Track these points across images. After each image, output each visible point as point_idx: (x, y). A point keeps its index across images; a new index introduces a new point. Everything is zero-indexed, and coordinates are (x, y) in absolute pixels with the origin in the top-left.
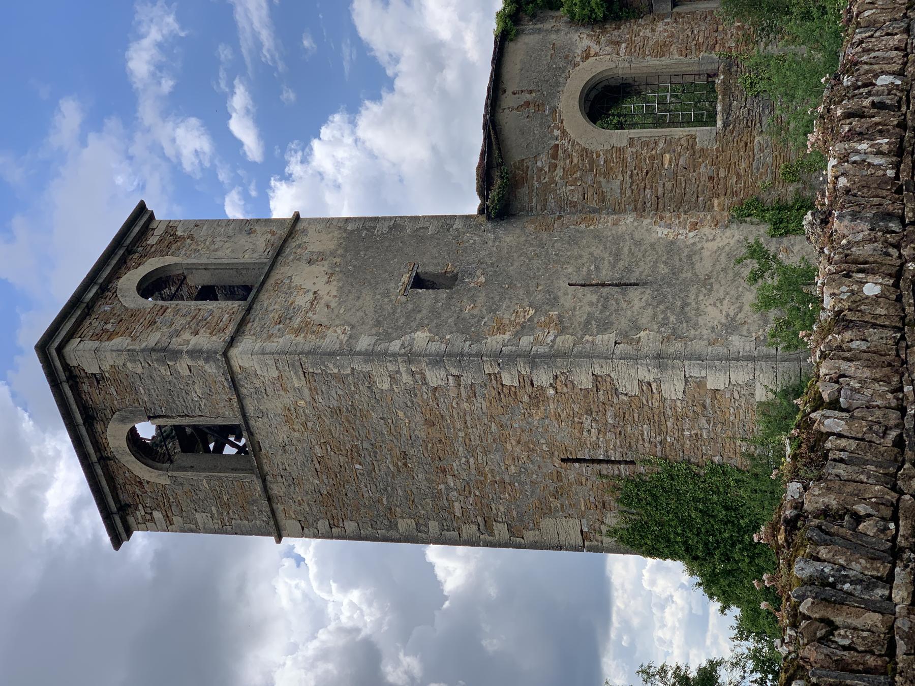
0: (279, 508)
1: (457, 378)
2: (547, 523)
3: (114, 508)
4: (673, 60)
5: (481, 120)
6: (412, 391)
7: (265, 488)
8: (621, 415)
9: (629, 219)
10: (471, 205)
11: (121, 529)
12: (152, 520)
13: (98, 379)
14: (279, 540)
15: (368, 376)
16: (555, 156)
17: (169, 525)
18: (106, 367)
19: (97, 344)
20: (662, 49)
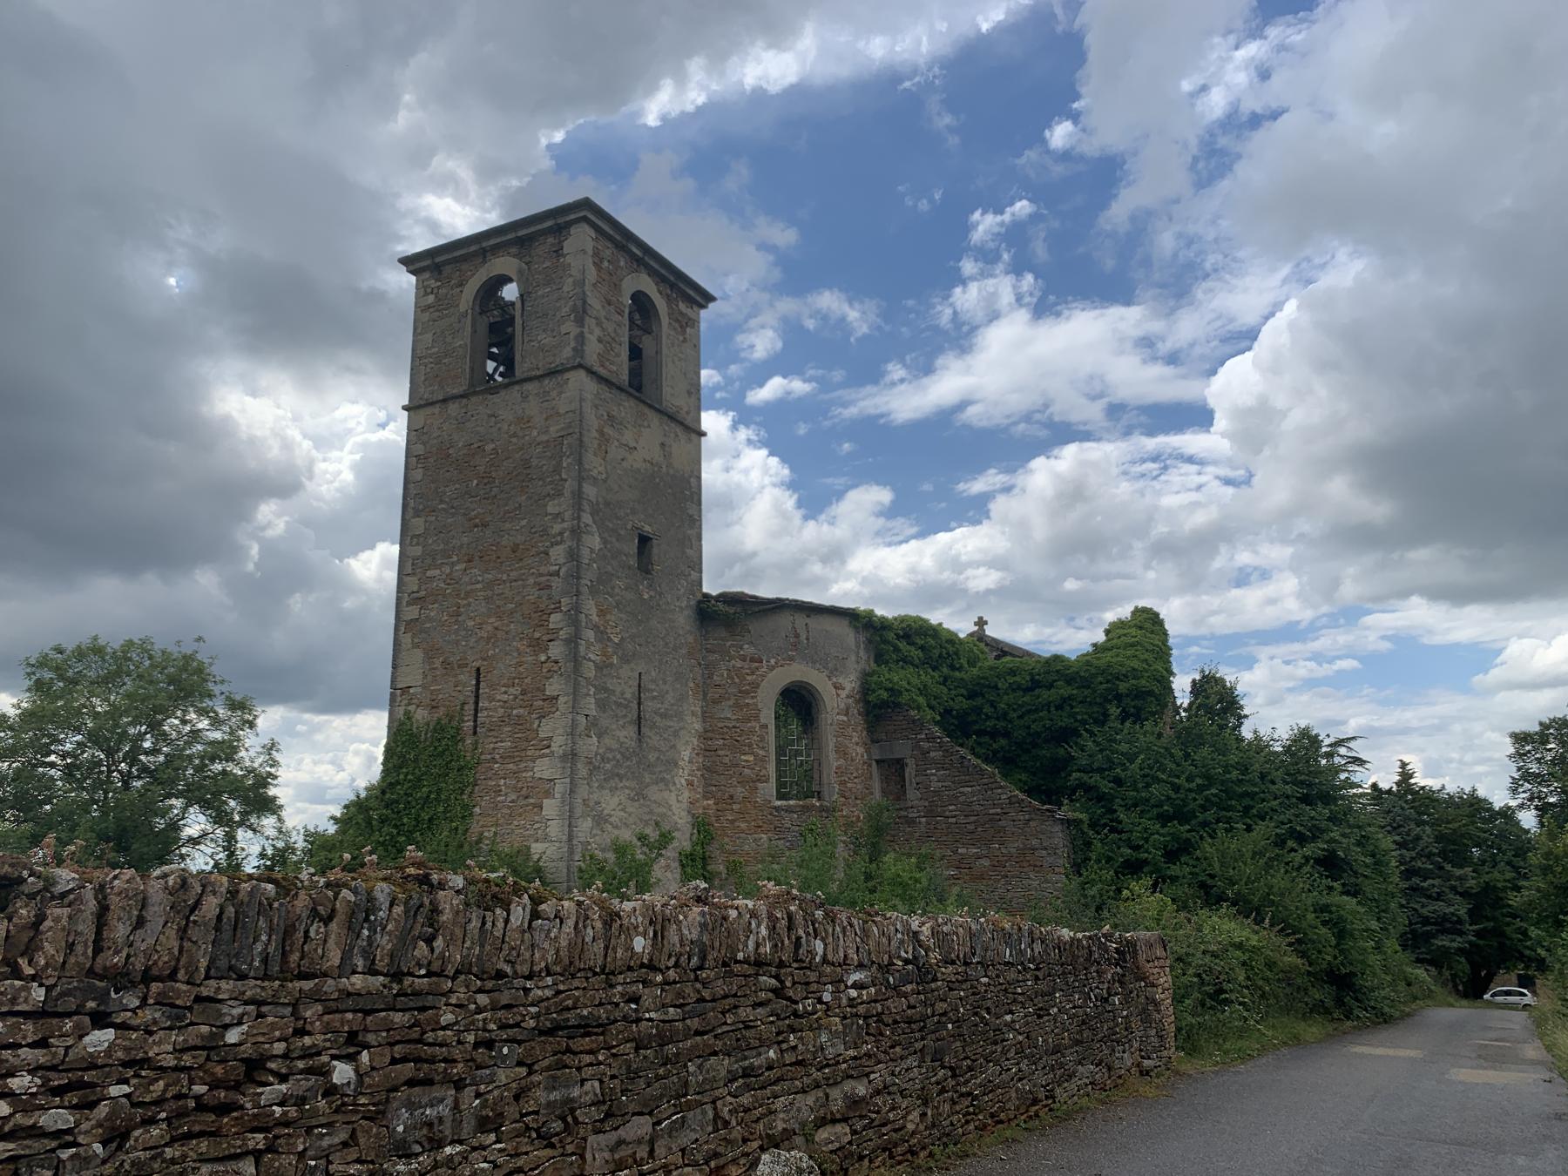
0: (436, 409)
1: (557, 574)
2: (419, 654)
3: (438, 260)
4: (832, 761)
5: (783, 596)
6: (545, 532)
7: (455, 398)
9: (698, 726)
10: (710, 587)
11: (418, 265)
12: (426, 294)
13: (558, 252)
14: (404, 408)
15: (560, 494)
16: (752, 660)
17: (420, 308)
18: (569, 259)
19: (590, 252)
20: (841, 751)
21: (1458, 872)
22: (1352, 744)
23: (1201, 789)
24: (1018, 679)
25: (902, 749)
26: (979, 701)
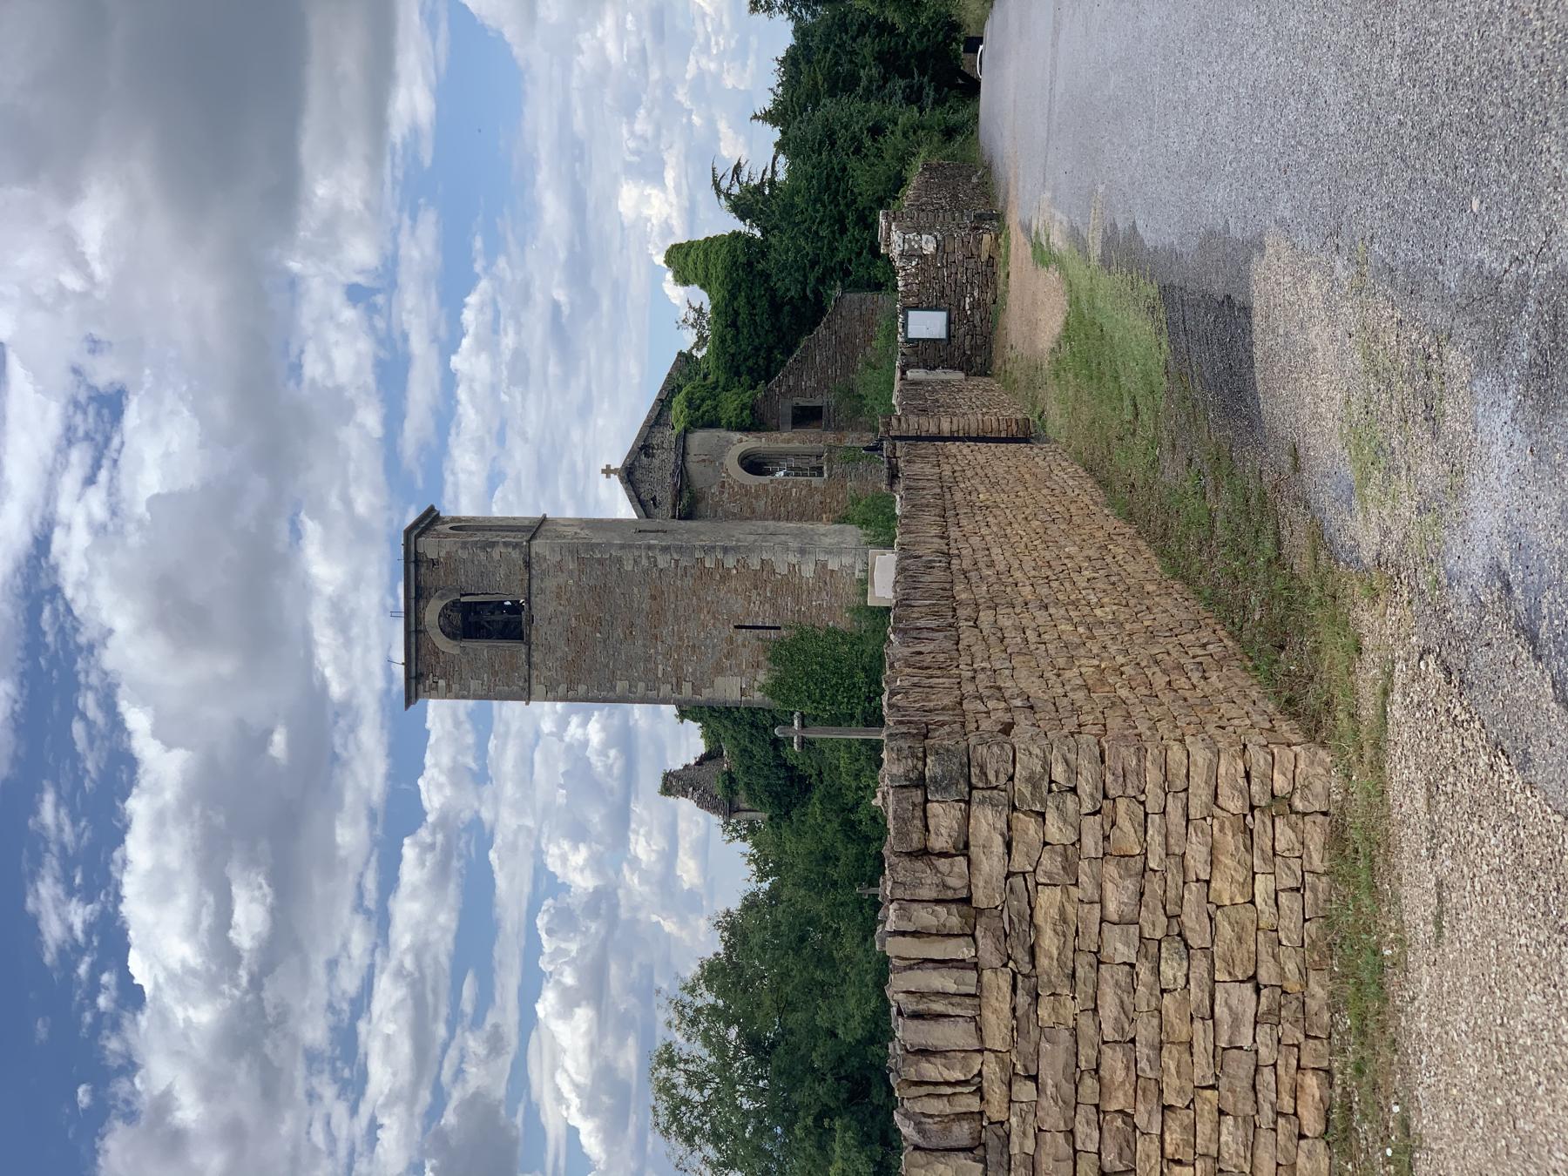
0: (534, 673)
2: (719, 681)
6: (646, 572)
7: (529, 655)
8: (774, 591)
13: (434, 563)
15: (620, 560)
16: (723, 486)
20: (789, 441)
21: (864, 83)
22: (719, 173)
23: (824, 206)
24: (729, 337)
25: (785, 407)
26: (743, 369)
